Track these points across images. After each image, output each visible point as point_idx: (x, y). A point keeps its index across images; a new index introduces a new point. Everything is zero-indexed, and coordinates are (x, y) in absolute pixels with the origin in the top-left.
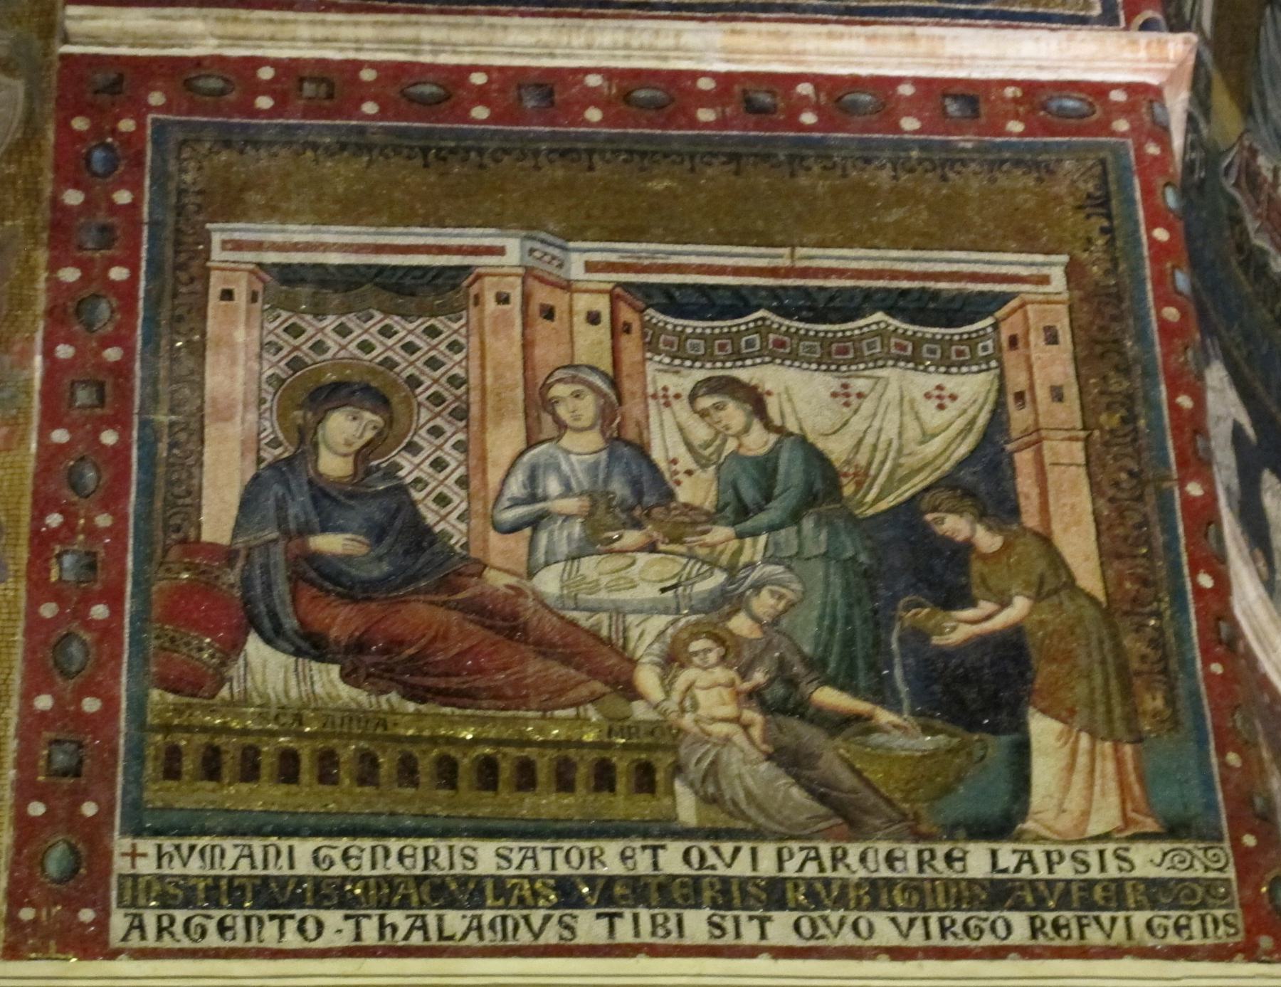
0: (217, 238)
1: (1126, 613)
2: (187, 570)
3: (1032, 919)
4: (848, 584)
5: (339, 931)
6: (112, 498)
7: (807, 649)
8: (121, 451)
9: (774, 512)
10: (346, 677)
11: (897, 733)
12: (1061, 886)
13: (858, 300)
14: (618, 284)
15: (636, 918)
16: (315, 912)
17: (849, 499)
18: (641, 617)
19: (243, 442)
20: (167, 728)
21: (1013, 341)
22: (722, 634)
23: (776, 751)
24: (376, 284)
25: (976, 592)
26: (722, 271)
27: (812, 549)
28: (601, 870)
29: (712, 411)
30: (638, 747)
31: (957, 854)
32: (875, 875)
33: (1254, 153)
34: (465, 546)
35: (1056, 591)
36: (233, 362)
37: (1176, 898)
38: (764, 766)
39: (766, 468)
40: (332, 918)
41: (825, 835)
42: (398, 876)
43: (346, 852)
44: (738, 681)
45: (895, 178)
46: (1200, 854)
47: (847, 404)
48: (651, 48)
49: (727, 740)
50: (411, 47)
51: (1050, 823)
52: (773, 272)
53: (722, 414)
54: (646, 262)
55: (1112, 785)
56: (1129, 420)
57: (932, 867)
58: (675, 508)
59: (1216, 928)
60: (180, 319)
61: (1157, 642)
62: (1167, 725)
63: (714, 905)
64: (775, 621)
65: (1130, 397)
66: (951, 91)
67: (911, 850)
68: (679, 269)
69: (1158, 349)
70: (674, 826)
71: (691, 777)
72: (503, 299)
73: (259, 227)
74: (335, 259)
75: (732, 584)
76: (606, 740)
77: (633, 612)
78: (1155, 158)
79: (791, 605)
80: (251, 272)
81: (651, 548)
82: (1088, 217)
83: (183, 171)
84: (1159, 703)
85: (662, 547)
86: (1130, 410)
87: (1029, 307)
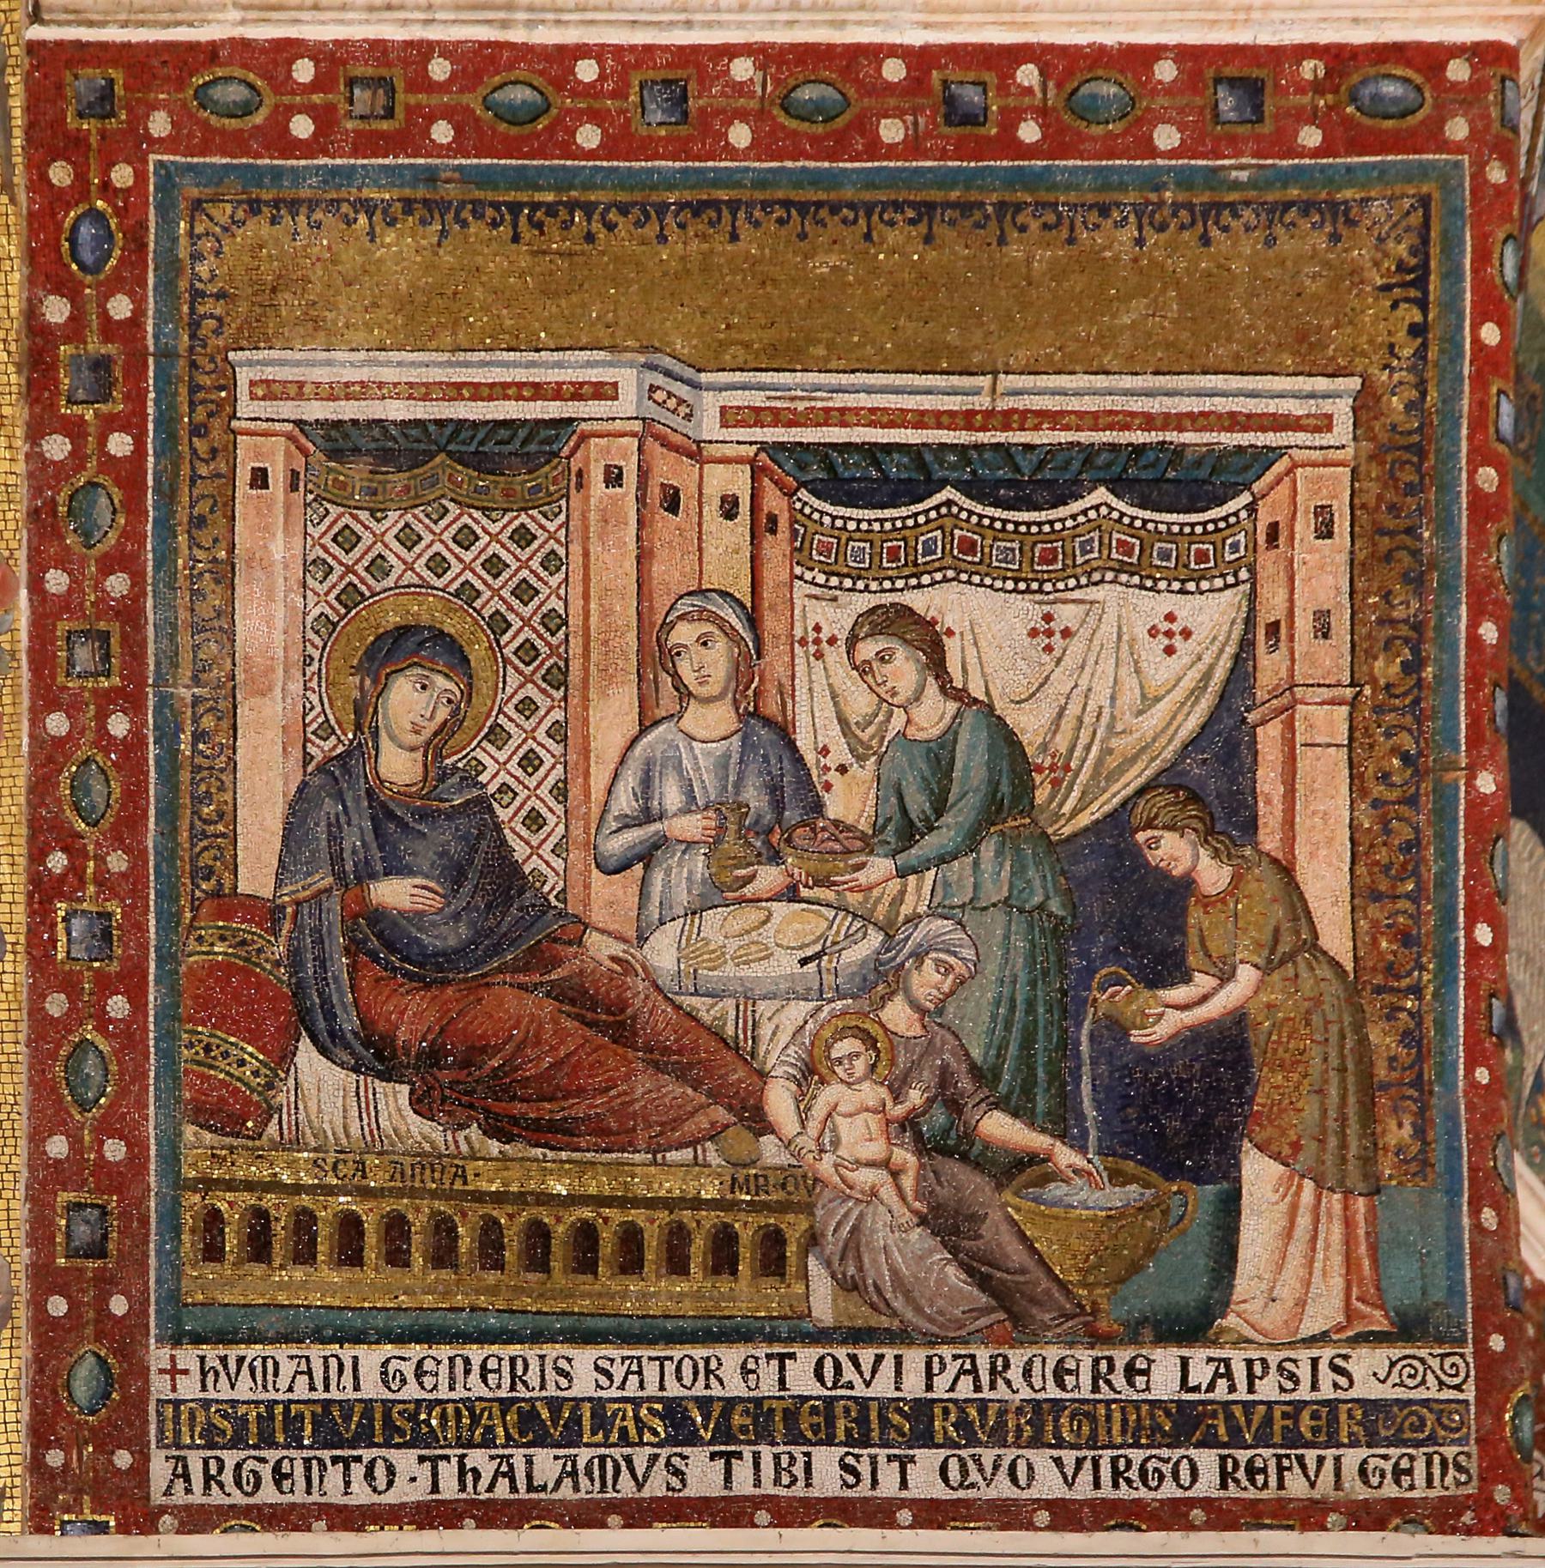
0: (244, 376)
1: (1378, 990)
2: (223, 939)
3: (1223, 1459)
4: (1032, 943)
5: (413, 1479)
6: (125, 831)
7: (976, 1053)
8: (133, 745)
10: (420, 1104)
11: (1079, 1181)
12: (1262, 1409)
13: (1076, 465)
14: (764, 446)
15: (757, 1457)
16: (383, 1452)
17: (1042, 809)
18: (777, 1003)
20: (208, 1184)
22: (875, 1030)
23: (932, 1209)
24: (450, 454)
25: (1192, 960)
27: (995, 892)
28: (716, 1391)
29: (875, 665)
31: (1141, 1364)
32: (1041, 1396)
34: (562, 896)
35: (1290, 957)
37: (1400, 1430)
40: (405, 1460)
41: (987, 1336)
42: (480, 1399)
43: (420, 1363)
44: (889, 1104)
45: (1140, 242)
46: (1435, 1363)
47: (1049, 649)
49: (874, 1193)
50: (502, 15)
51: (1255, 1318)
52: (968, 419)
53: (888, 668)
54: (801, 406)
55: (1337, 1260)
57: (1108, 1383)
58: (823, 829)
59: (1444, 1474)
62: (1413, 1167)
63: (849, 1442)
65: (1418, 627)
67: (1085, 1357)
68: (843, 417)
69: (1464, 542)
70: (807, 1325)
71: (829, 1249)
72: (614, 477)
73: (298, 356)
74: (397, 411)
75: (888, 950)
76: (729, 1196)
77: (765, 998)
80: (290, 437)
81: (791, 894)
82: (1395, 306)
83: (197, 257)
84: (1407, 1130)
85: (805, 892)
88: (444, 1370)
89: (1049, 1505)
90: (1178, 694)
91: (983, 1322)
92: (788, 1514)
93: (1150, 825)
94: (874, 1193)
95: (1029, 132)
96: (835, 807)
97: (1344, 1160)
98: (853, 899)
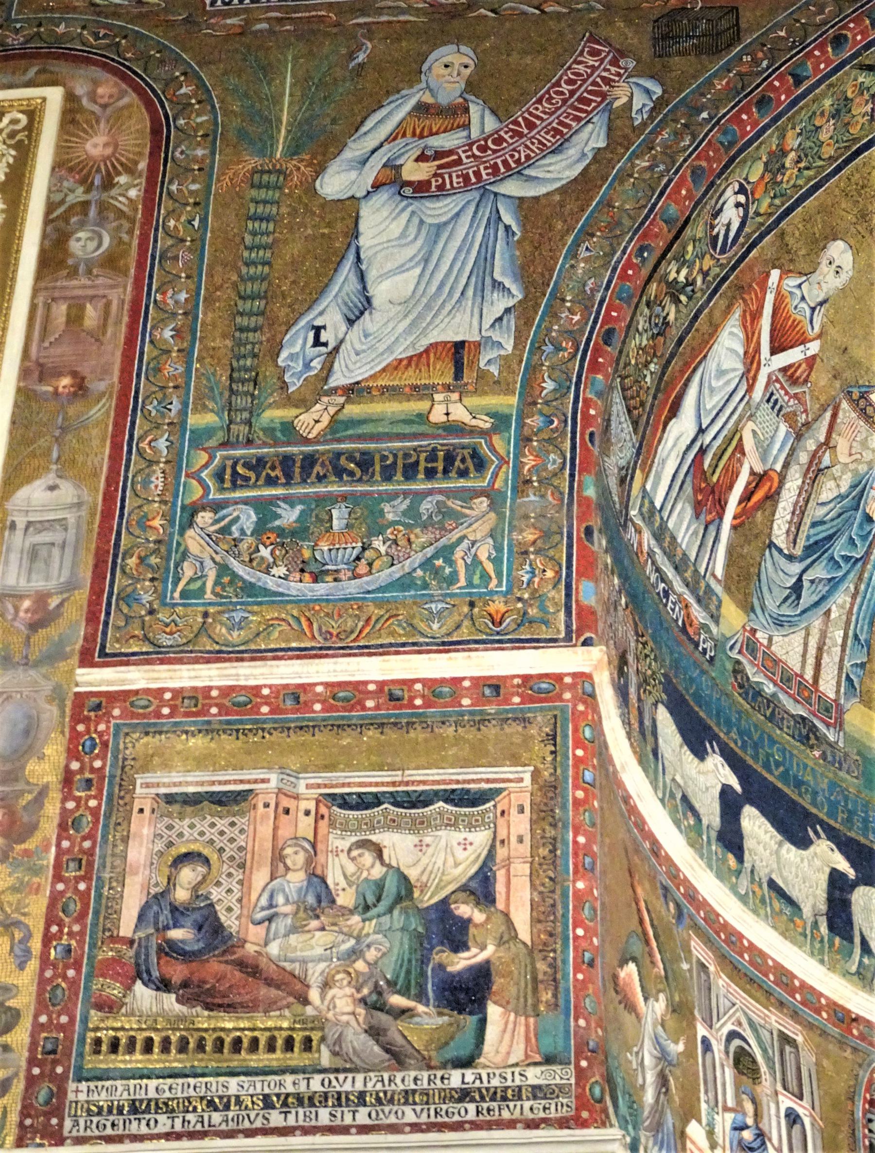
0: (139, 782)
1: (540, 951)
7: (388, 976)
9: (382, 907)
10: (178, 1001)
14: (321, 795)
15: (297, 1113)
19: (142, 885)
20: (97, 1029)
21: (503, 813)
25: (470, 944)
26: (370, 784)
27: (397, 925)
28: (283, 1090)
30: (305, 1029)
31: (446, 1076)
33: (754, 631)
34: (238, 932)
35: (507, 942)
36: (141, 845)
38: (363, 1036)
39: (380, 886)
40: (162, 1118)
41: (388, 1069)
46: (559, 1072)
48: (346, 671)
49: (348, 1023)
52: (394, 784)
55: (522, 1039)
56: (553, 851)
60: (119, 824)
61: (553, 966)
63: (334, 1106)
64: (376, 963)
65: (555, 839)
66: (488, 683)
67: (425, 1074)
69: (571, 813)
72: (267, 805)
74: (191, 789)
78: (581, 712)
79: (384, 954)
81: (323, 929)
86: (554, 846)
87: (512, 795)
88: (180, 1088)
89: (410, 1125)
90: (468, 862)
91: (387, 1064)
92: (307, 1131)
93: (456, 902)
94: (348, 1023)
95: (418, 702)
96: (340, 901)
97: (526, 1006)
98: (345, 930)
